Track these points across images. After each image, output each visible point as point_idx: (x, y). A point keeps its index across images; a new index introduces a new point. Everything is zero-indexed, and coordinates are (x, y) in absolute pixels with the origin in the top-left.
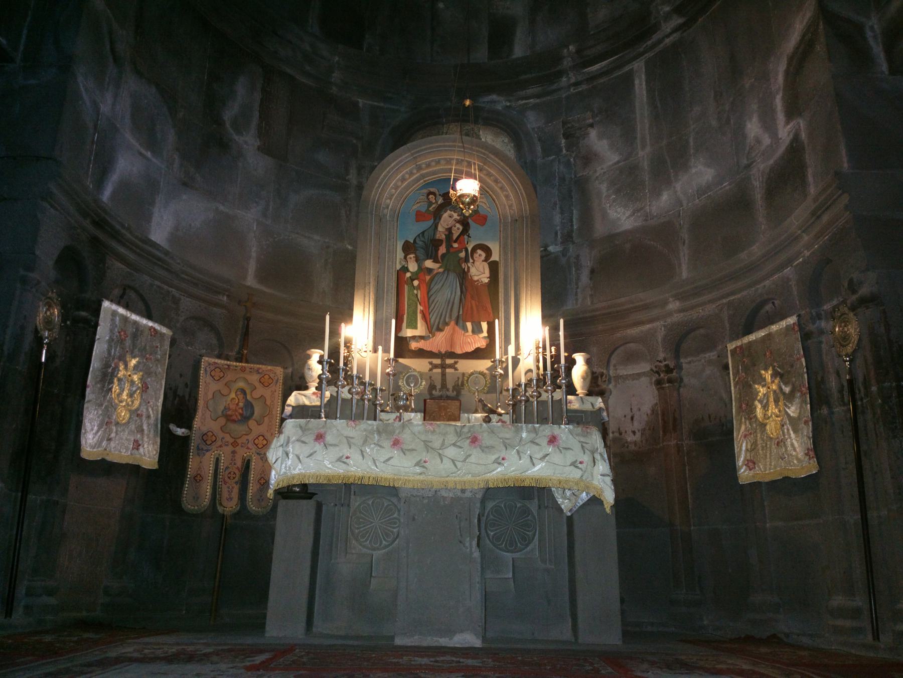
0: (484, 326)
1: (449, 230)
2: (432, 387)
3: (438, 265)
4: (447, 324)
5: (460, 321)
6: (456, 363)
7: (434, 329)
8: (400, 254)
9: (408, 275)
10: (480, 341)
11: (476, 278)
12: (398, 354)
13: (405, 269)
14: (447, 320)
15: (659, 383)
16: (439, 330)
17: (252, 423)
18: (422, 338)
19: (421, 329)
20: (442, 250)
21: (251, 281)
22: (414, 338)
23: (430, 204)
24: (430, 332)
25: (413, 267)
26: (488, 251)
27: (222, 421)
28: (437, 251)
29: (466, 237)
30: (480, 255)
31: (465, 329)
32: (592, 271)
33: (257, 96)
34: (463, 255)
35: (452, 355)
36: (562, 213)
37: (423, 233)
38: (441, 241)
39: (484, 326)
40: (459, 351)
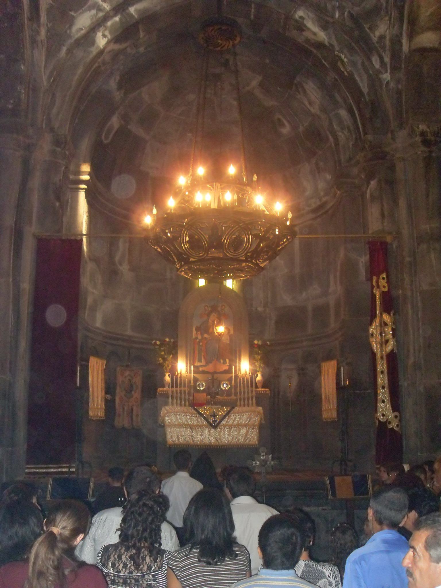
0: (227, 361)
5: (218, 360)
7: (208, 362)
8: (194, 332)
9: (198, 340)
10: (225, 367)
12: (194, 372)
13: (196, 338)
15: (299, 374)
16: (210, 362)
17: (133, 392)
19: (203, 363)
21: (129, 332)
22: (201, 366)
25: (200, 337)
27: (124, 393)
31: (221, 363)
33: (127, 245)
35: (215, 373)
39: (227, 361)
40: (218, 371)
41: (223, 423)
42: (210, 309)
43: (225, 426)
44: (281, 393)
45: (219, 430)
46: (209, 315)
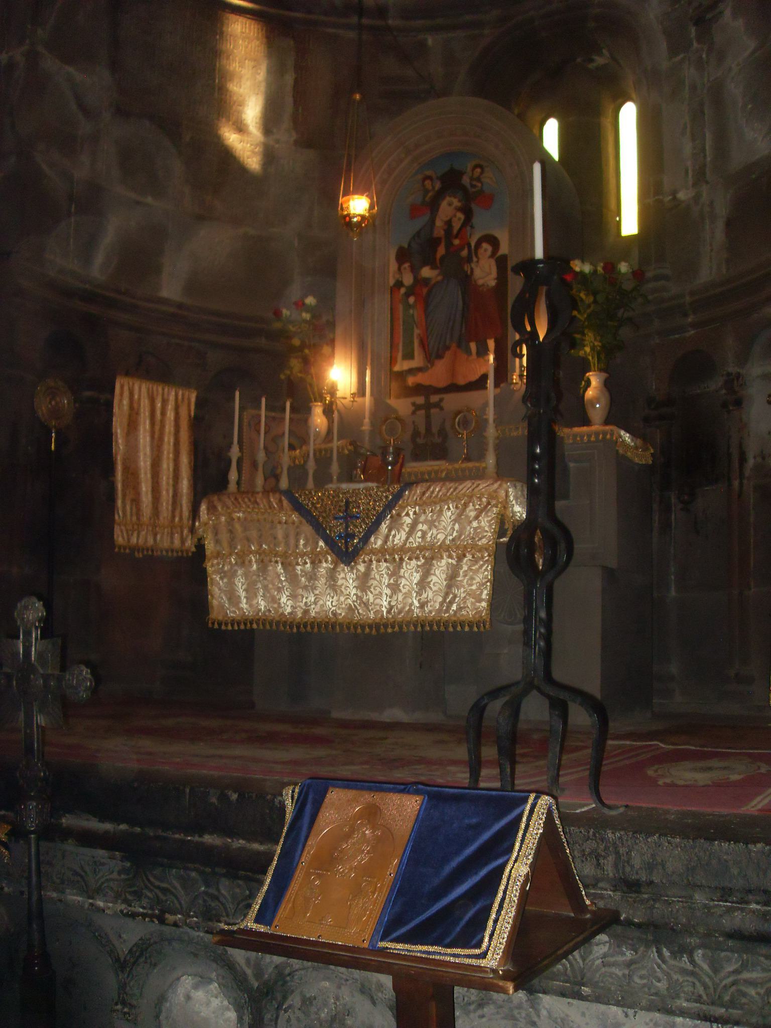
0: (491, 344)
1: (449, 223)
2: (416, 434)
3: (436, 272)
4: (448, 348)
5: (462, 344)
6: (441, 400)
7: (432, 356)
8: (393, 265)
9: (403, 290)
11: (480, 282)
14: (448, 343)
16: (440, 356)
18: (420, 370)
19: (417, 361)
20: (441, 251)
22: (411, 371)
23: (427, 191)
24: (429, 361)
26: (494, 242)
28: (435, 251)
29: (468, 228)
30: (486, 250)
31: (468, 352)
32: (729, 223)
34: (465, 253)
36: (693, 140)
37: (418, 234)
38: (439, 239)
39: (491, 344)
40: (461, 382)
41: (376, 542)
42: (438, 185)
43: (384, 553)
44: (751, 462)
45: (362, 568)
46: (433, 205)
